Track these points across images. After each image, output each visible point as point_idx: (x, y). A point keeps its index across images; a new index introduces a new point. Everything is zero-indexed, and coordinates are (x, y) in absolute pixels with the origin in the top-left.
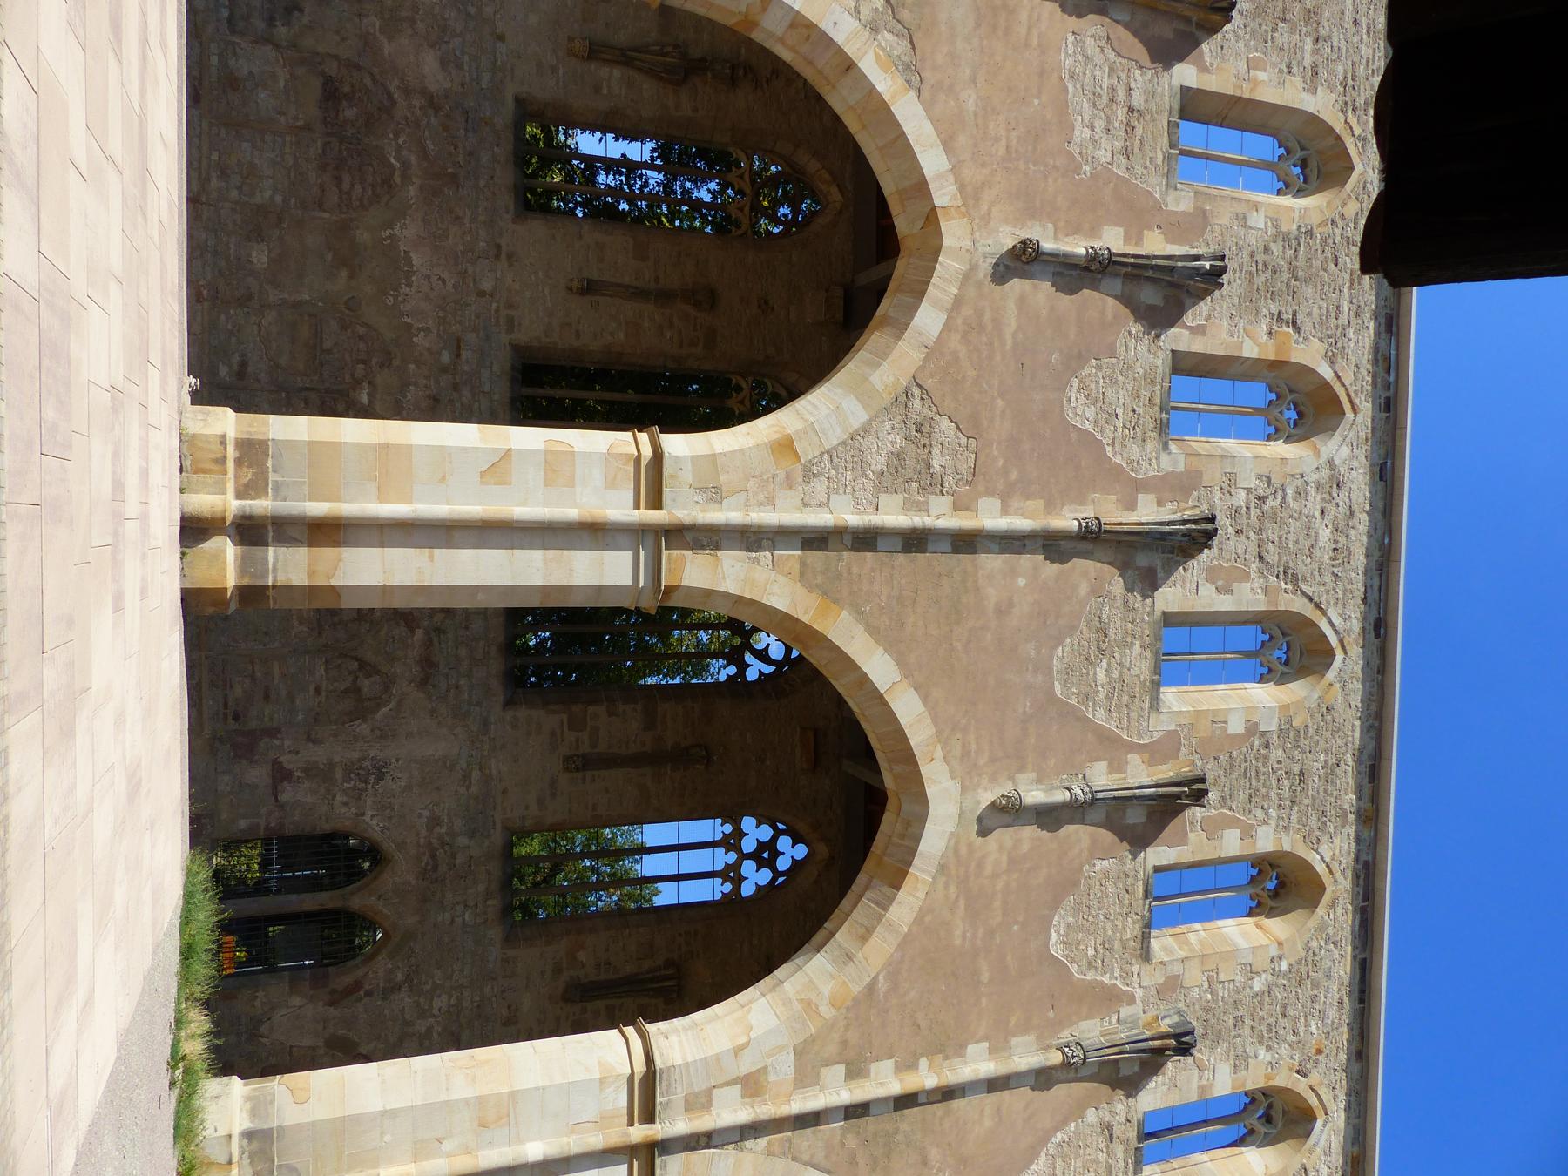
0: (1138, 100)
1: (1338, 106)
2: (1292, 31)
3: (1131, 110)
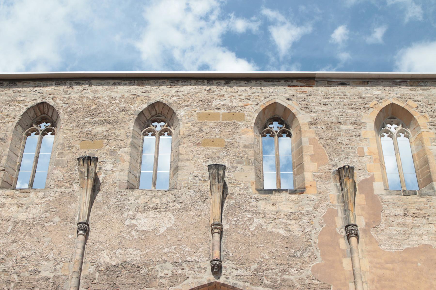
0: (400, 212)
1: (367, 112)
2: (339, 135)
3: (405, 215)
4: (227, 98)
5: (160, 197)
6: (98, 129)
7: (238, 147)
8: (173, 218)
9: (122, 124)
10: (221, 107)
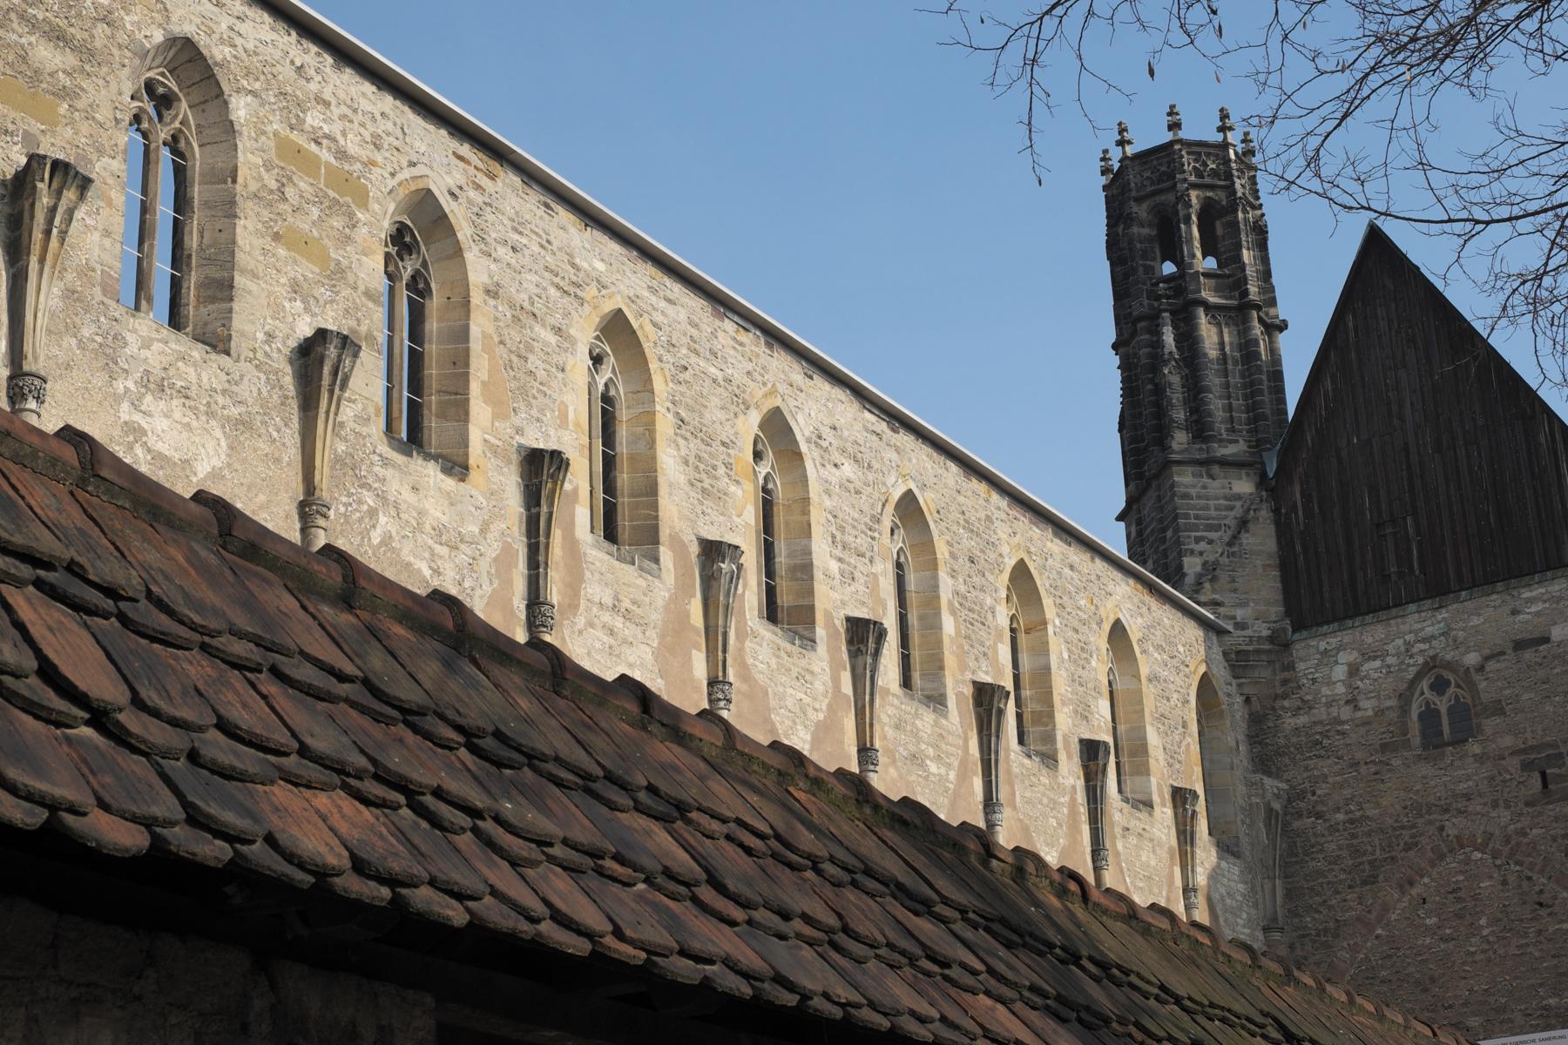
4: (335, 117)
5: (195, 365)
6: (46, 55)
7: (355, 289)
8: (223, 443)
9: (105, 69)
10: (325, 142)
